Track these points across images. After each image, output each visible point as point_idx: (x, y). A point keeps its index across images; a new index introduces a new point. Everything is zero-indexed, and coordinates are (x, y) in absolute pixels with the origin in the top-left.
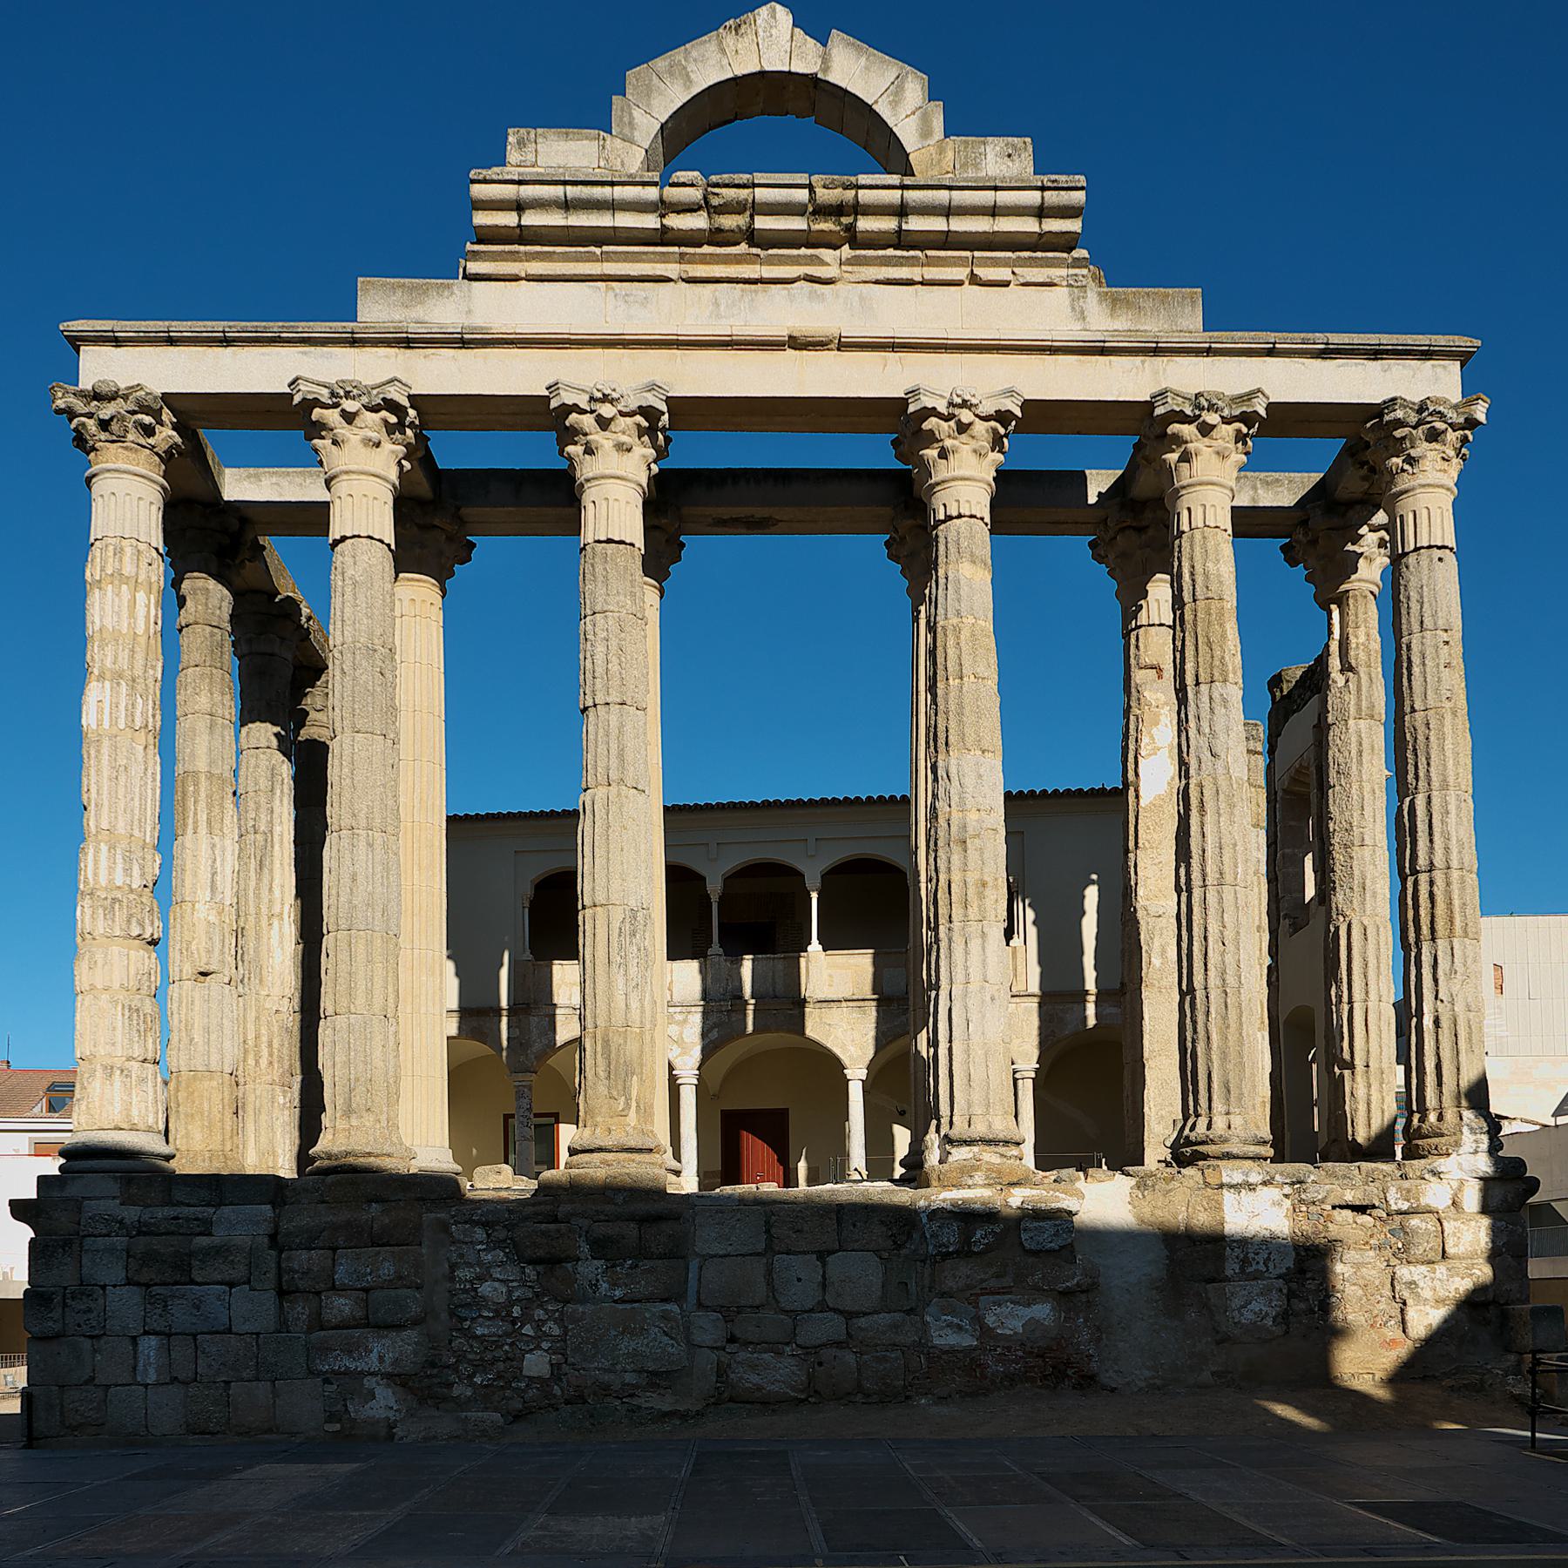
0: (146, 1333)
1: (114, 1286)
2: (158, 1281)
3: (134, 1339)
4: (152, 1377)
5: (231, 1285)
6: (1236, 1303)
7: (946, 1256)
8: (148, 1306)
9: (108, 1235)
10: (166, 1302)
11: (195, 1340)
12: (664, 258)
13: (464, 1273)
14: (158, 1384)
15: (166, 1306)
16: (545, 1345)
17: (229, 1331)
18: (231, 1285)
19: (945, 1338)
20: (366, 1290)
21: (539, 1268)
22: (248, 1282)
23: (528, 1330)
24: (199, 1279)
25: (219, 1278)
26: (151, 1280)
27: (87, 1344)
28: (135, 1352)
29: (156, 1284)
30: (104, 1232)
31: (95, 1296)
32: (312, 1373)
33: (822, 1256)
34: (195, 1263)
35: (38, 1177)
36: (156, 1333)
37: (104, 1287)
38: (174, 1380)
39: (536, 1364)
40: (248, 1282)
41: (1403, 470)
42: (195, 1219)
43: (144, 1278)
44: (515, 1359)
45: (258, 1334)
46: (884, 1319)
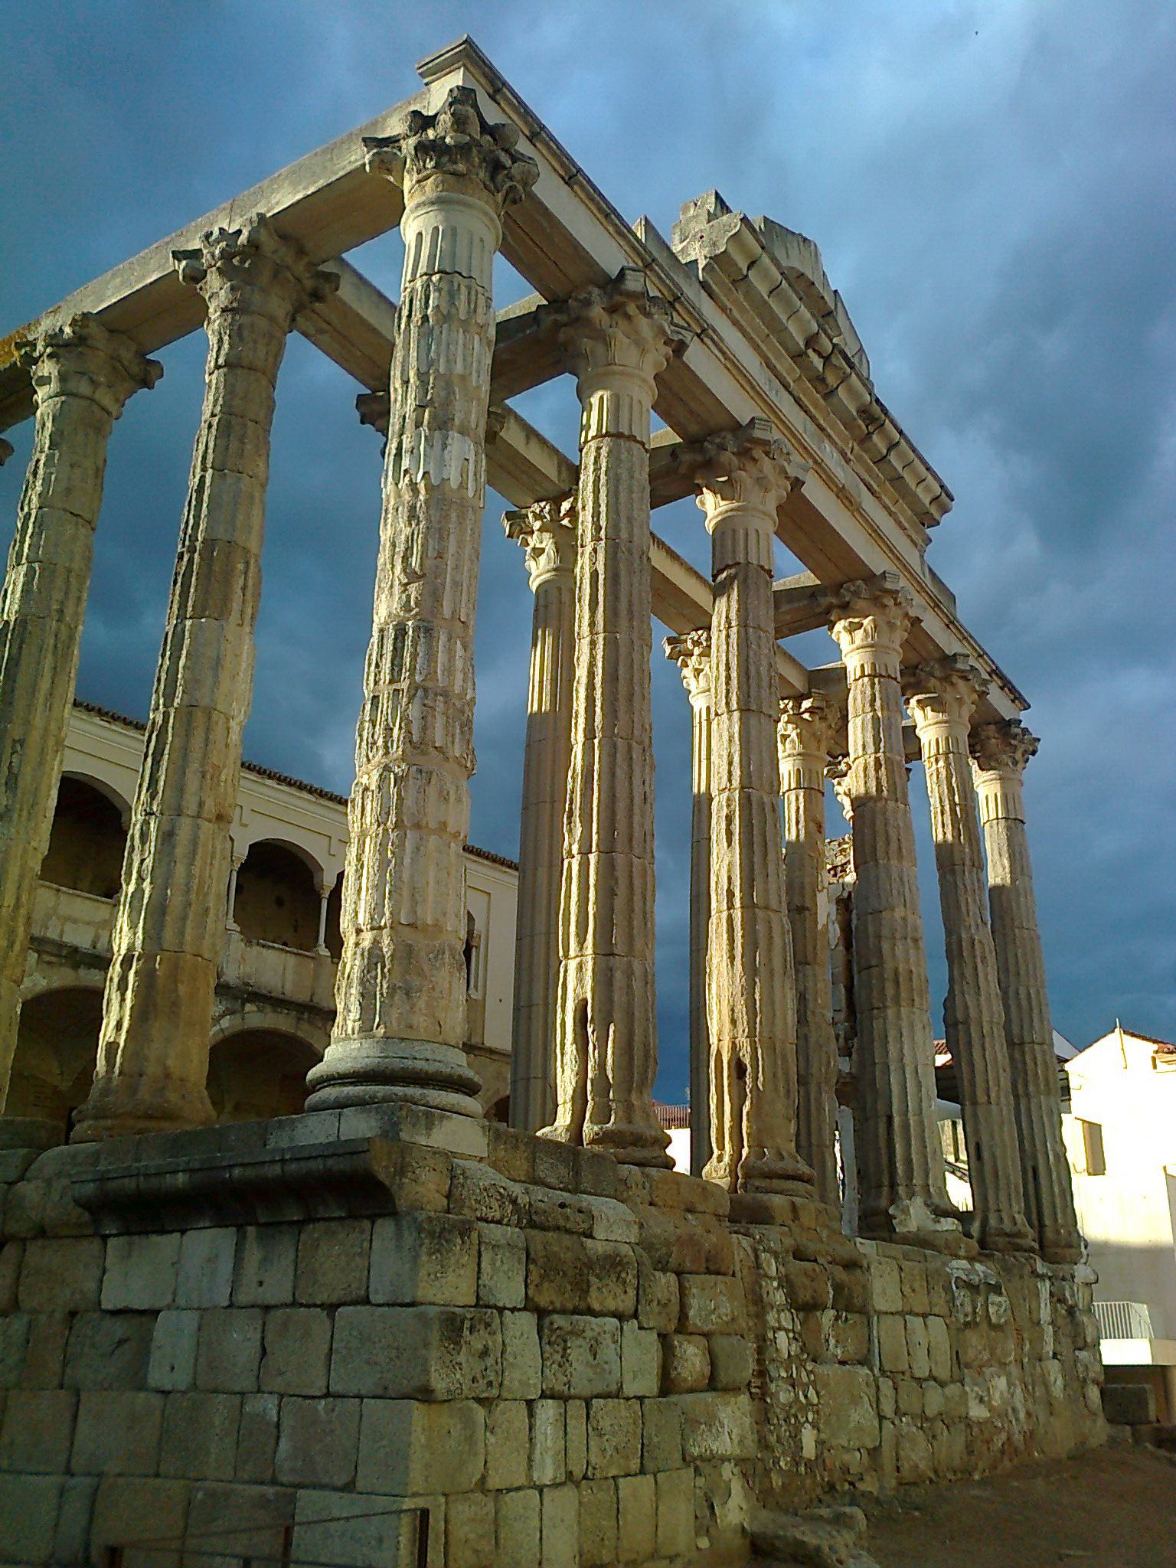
1: (513, 1310)
2: (558, 1305)
3: (530, 1403)
4: (547, 1472)
5: (620, 1316)
7: (967, 1324)
8: (547, 1348)
9: (499, 1222)
10: (565, 1341)
11: (588, 1406)
12: (790, 371)
13: (771, 1318)
14: (555, 1485)
15: (565, 1349)
17: (617, 1395)
18: (620, 1316)
22: (635, 1315)
23: (802, 1398)
24: (596, 1306)
25: (611, 1304)
26: (552, 1303)
27: (480, 1412)
29: (555, 1311)
30: (498, 1215)
31: (494, 1326)
32: (686, 1459)
33: (925, 1316)
34: (593, 1279)
35: (1100, 1126)
37: (501, 1310)
40: (635, 1315)
41: (1007, 765)
42: (580, 1211)
43: (543, 1301)
45: (641, 1399)
46: (953, 1389)
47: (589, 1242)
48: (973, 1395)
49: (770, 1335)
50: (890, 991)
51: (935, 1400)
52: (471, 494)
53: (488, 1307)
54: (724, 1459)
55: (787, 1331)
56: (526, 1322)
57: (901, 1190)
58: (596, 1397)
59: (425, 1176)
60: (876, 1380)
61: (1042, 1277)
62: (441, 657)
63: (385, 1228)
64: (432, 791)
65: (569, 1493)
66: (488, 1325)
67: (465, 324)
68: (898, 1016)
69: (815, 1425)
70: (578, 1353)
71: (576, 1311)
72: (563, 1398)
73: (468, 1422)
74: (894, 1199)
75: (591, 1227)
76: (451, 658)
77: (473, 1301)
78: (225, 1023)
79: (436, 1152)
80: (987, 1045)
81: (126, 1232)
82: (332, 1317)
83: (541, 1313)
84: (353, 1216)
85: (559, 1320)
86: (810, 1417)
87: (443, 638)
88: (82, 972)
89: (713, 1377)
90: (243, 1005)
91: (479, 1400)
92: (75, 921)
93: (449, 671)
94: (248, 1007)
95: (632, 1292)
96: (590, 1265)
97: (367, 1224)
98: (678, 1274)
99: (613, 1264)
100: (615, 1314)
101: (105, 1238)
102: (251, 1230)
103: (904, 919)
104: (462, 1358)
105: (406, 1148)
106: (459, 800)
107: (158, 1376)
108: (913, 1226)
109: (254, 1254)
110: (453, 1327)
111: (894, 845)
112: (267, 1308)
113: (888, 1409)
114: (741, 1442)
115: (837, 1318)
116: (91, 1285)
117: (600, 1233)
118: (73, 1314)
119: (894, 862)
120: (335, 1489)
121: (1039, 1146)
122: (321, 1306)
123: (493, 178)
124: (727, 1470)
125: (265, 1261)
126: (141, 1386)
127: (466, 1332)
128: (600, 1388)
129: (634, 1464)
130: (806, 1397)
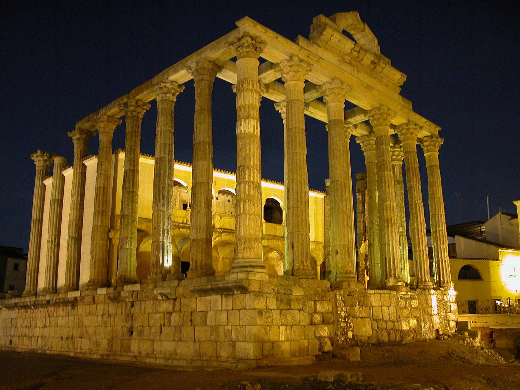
0: (282, 325)
1: (274, 309)
3: (279, 327)
5: (299, 310)
6: (435, 320)
13: (339, 309)
14: (285, 341)
16: (351, 329)
19: (405, 327)
20: (322, 313)
21: (349, 308)
22: (303, 310)
24: (293, 308)
28: (279, 331)
34: (292, 303)
36: (284, 325)
37: (271, 310)
38: (288, 340)
39: (350, 335)
40: (303, 310)
42: (289, 290)
43: (281, 307)
44: (347, 333)
45: (304, 326)
47: (291, 296)
48: (404, 324)
49: (339, 312)
50: (386, 225)
51: (390, 325)
52: (256, 133)
53: (268, 309)
54: (325, 337)
55: (344, 311)
56: (277, 312)
57: (388, 276)
58: (294, 325)
59: (254, 285)
60: (371, 321)
61: (434, 294)
62: (251, 174)
63: (247, 295)
64: (252, 204)
65: (288, 343)
66: (269, 312)
67: (251, 91)
68: (388, 231)
69: (352, 331)
70: (289, 317)
71: (288, 309)
72: (286, 325)
73: (266, 329)
74: (387, 278)
75: (292, 293)
76: (254, 174)
77: (265, 308)
78: (217, 239)
79: (256, 280)
80: (420, 234)
81: (200, 296)
82: (239, 312)
83: (281, 310)
84: (241, 293)
85: (284, 311)
86: (351, 329)
87: (252, 170)
88: (181, 229)
89: (323, 321)
90: (221, 234)
91: (268, 326)
92: (178, 217)
93: (254, 177)
94: (222, 234)
95: (301, 305)
96: (291, 300)
97: (244, 295)
98: (314, 301)
99: (297, 300)
100: (298, 310)
101: (196, 297)
102: (223, 296)
103: (390, 205)
104: (263, 318)
105: (250, 280)
106: (257, 206)
107: (209, 323)
108: (391, 284)
109: (224, 300)
110: (261, 312)
111: (387, 184)
112: (228, 310)
113: (375, 327)
114: (330, 333)
115: (360, 308)
116: (194, 307)
117: (294, 294)
118: (192, 312)
119: (387, 189)
120: (242, 341)
121: (440, 259)
122: (238, 310)
123: (256, 50)
124: (326, 340)
125: (227, 301)
126: (206, 325)
127: (264, 313)
128: (294, 323)
129: (303, 338)
130: (350, 325)
